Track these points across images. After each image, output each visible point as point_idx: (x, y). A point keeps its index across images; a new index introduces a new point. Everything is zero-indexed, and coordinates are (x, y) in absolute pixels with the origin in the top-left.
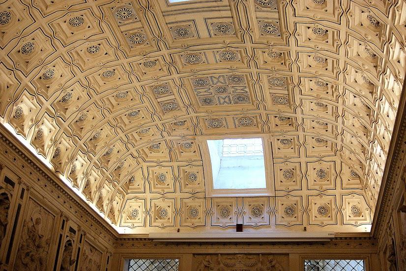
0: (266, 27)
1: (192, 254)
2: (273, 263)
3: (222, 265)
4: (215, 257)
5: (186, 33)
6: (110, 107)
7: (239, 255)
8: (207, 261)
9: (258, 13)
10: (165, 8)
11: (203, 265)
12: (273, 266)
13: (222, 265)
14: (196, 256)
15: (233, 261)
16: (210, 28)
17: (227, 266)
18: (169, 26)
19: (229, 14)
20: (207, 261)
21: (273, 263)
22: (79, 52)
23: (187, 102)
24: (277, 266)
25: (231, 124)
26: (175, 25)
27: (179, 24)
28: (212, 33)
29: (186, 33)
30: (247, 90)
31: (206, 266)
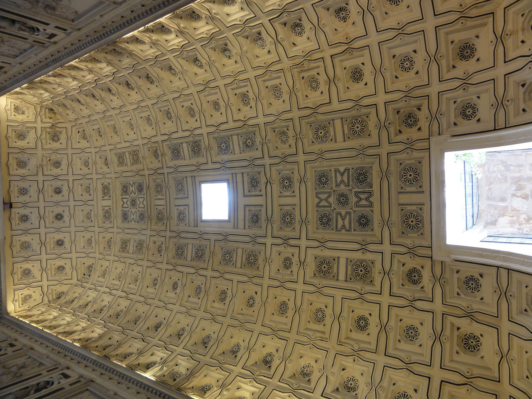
0: (248, 145)
5: (257, 216)
6: (319, 335)
9: (236, 152)
10: (231, 225)
16: (253, 193)
18: (247, 227)
19: (239, 176)
22: (241, 312)
23: (357, 246)
25: (416, 198)
26: (247, 223)
27: (247, 219)
28: (258, 193)
29: (257, 216)
30: (342, 169)
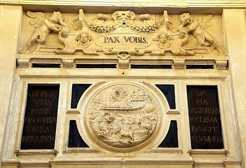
1: (19, 10)
2: (191, 27)
3: (85, 29)
4: (70, 18)
7: (120, 13)
8: (54, 22)
11: (44, 28)
12: (191, 33)
13: (85, 29)
14: (29, 13)
15: (109, 24)
17: (97, 30)
20: (54, 22)
21: (191, 27)
24: (198, 31)
31: (52, 32)
